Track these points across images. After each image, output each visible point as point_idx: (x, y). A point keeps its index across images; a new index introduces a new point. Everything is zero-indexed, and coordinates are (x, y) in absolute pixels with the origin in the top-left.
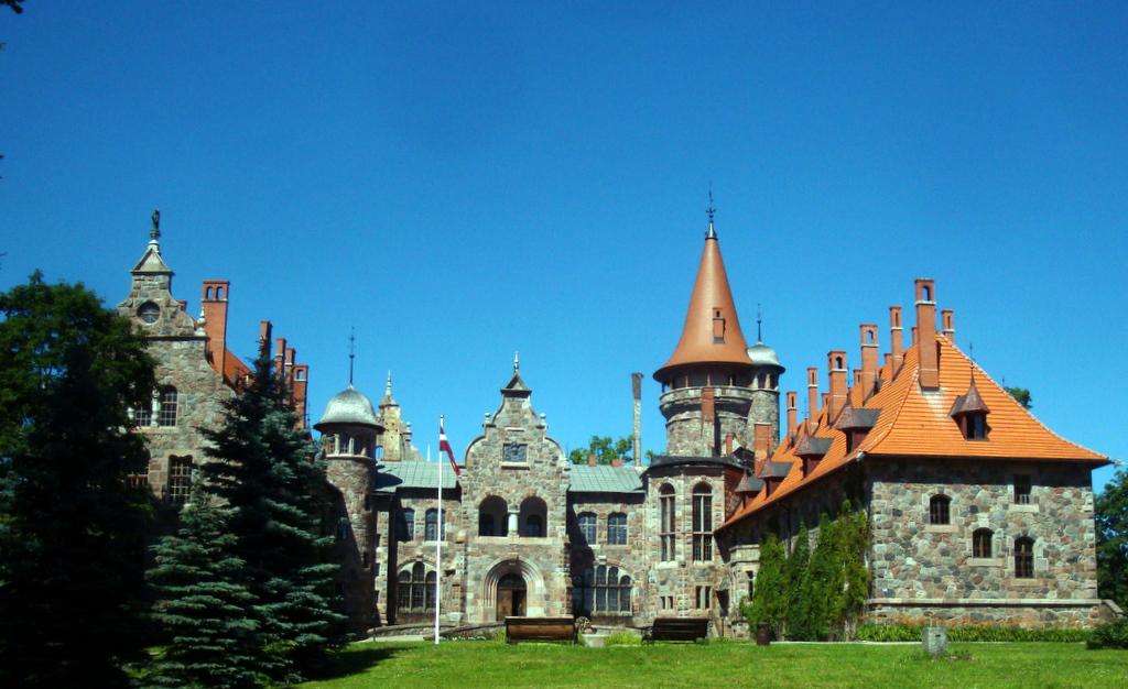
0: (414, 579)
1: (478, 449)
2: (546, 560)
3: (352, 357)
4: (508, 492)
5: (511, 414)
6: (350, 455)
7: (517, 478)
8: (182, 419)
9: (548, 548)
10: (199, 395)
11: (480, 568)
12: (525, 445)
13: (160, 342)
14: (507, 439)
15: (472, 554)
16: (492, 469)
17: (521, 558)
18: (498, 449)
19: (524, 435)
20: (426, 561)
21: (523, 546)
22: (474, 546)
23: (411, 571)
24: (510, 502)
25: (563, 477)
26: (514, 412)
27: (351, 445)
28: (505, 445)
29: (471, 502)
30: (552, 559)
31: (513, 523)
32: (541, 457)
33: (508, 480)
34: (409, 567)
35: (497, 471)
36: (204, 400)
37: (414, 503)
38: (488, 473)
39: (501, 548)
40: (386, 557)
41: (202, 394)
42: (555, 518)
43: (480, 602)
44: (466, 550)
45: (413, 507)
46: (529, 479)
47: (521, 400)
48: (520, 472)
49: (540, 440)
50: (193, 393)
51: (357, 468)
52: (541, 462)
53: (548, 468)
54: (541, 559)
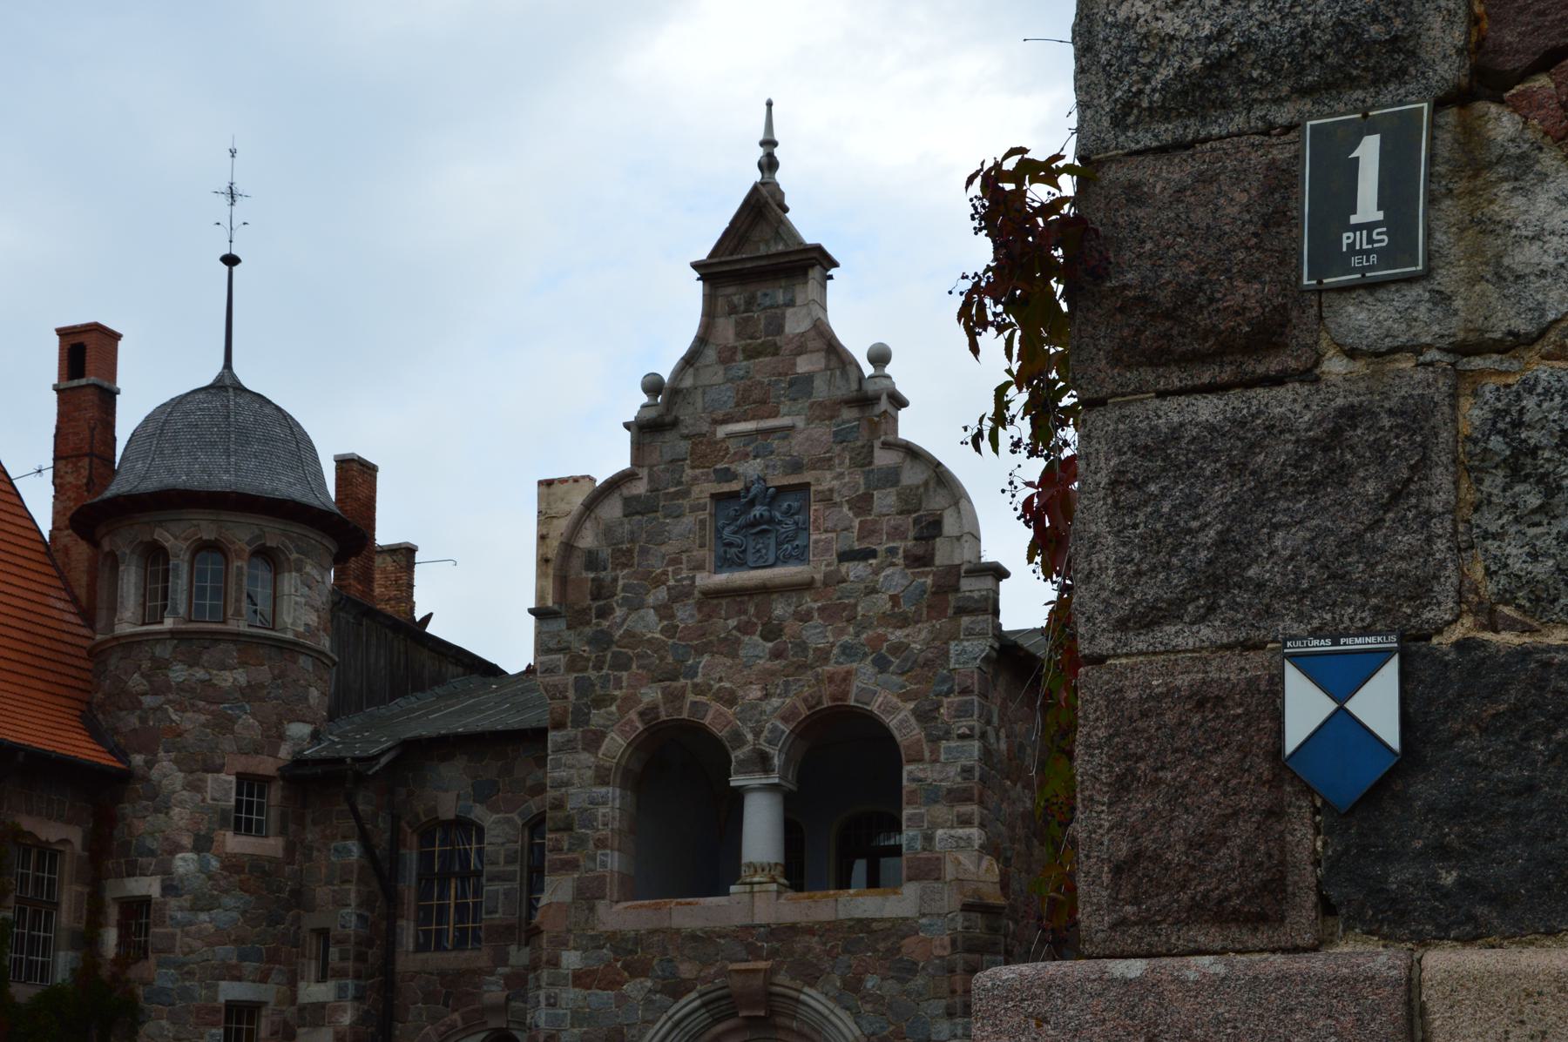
1: (608, 532)
2: (891, 987)
4: (730, 699)
5: (741, 365)
6: (169, 623)
7: (765, 638)
9: (899, 929)
12: (805, 487)
14: (727, 475)
15: (581, 979)
16: (664, 611)
19: (797, 446)
21: (793, 929)
22: (596, 942)
24: (738, 739)
25: (961, 611)
26: (751, 354)
27: (180, 584)
28: (716, 497)
29: (586, 758)
30: (919, 981)
32: (867, 532)
33: (730, 646)
35: (685, 615)
38: (649, 624)
39: (701, 941)
42: (932, 795)
44: (555, 963)
47: (780, 297)
48: (780, 609)
49: (864, 459)
51: (200, 674)
52: (873, 554)
53: (895, 578)
54: (871, 982)
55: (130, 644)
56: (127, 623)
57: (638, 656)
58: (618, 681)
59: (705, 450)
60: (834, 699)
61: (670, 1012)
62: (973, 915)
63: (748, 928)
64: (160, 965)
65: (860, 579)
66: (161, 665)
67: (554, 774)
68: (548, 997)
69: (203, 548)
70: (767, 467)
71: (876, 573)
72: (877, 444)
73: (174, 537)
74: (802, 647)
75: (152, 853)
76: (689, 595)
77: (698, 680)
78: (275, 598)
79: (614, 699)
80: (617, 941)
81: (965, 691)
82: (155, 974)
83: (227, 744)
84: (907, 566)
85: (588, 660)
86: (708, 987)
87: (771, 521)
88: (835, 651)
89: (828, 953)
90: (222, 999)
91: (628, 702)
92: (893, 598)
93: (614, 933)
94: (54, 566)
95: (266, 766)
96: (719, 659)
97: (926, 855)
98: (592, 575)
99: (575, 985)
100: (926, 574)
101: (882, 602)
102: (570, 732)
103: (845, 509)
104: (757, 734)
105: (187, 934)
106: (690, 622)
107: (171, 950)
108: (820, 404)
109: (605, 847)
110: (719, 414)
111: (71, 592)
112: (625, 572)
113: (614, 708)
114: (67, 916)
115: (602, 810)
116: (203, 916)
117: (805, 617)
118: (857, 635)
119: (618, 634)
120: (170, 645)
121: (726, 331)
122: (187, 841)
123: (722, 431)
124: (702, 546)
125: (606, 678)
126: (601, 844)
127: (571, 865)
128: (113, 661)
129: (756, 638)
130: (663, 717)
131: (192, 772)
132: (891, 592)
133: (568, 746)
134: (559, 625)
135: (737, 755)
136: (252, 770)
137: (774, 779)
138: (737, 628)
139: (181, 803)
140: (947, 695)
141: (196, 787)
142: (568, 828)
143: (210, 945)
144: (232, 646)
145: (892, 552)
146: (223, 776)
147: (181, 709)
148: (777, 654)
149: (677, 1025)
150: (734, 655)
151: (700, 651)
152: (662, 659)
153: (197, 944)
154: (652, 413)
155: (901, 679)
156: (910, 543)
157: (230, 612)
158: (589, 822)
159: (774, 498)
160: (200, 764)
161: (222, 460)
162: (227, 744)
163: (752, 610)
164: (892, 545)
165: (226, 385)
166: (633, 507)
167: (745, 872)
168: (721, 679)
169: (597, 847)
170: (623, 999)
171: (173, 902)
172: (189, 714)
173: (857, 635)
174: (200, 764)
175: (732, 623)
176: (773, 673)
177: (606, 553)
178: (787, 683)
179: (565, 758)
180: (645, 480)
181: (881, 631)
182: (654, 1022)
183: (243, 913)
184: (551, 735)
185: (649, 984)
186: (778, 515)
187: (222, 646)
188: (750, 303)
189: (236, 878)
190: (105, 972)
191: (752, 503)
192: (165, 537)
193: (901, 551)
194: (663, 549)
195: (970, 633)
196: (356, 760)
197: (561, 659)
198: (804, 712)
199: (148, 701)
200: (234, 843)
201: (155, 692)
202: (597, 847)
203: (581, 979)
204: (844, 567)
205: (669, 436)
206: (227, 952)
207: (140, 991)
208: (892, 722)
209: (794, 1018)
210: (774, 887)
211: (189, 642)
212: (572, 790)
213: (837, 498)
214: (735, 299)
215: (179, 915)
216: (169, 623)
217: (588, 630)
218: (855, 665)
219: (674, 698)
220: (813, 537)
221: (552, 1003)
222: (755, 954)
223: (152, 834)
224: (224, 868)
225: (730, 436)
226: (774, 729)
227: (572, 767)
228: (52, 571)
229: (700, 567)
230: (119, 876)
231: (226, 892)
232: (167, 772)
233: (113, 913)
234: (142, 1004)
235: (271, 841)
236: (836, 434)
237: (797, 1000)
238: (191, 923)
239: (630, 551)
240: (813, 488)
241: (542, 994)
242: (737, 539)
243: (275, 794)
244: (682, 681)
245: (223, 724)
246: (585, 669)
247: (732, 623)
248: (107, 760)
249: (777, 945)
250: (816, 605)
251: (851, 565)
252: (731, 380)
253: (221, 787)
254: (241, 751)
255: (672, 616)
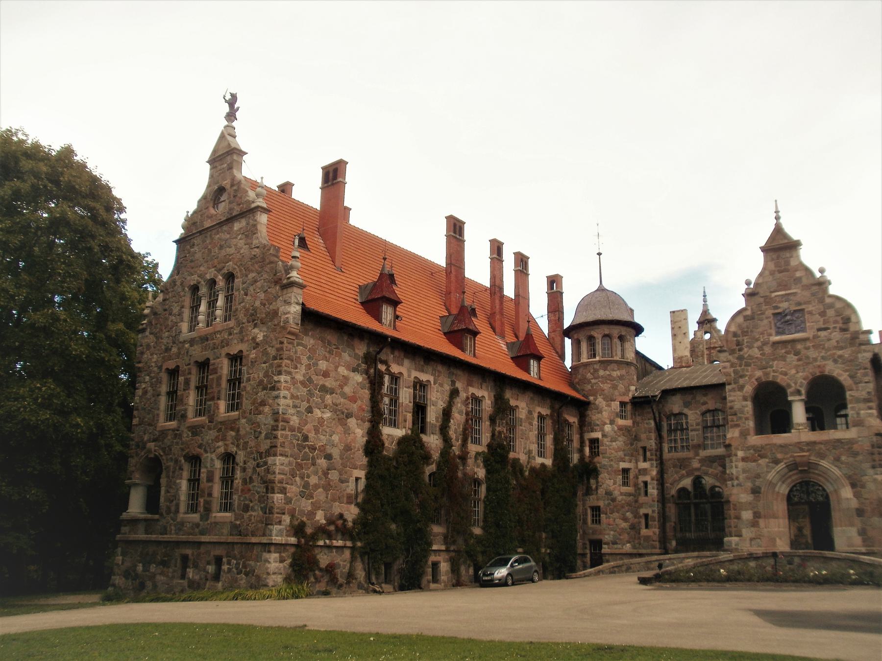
0: (696, 498)
1: (740, 326)
3: (599, 254)
4: (785, 374)
5: (778, 275)
6: (597, 359)
7: (795, 355)
8: (237, 310)
10: (251, 275)
11: (758, 476)
12: (803, 310)
13: (225, 228)
14: (776, 308)
15: (744, 459)
16: (760, 348)
17: (813, 459)
18: (766, 322)
19: (798, 298)
20: (706, 474)
21: (814, 443)
22: (749, 448)
23: (690, 488)
24: (789, 386)
26: (780, 272)
27: (599, 348)
28: (775, 315)
29: (739, 393)
31: (799, 414)
32: (825, 322)
33: (783, 358)
34: (687, 483)
35: (768, 349)
36: (256, 281)
37: (687, 405)
38: (756, 352)
39: (783, 447)
40: (654, 473)
41: (254, 275)
43: (762, 522)
44: (736, 455)
45: (686, 411)
46: (812, 353)
47: (788, 255)
48: (799, 346)
49: (821, 301)
50: (247, 276)
51: (608, 373)
53: (836, 336)
55: (586, 365)
56: (584, 359)
57: (753, 362)
58: (747, 371)
59: (768, 300)
60: (820, 372)
61: (776, 469)
62: (878, 437)
63: (799, 443)
64: (603, 457)
65: (826, 336)
66: (596, 371)
67: (729, 398)
68: (736, 465)
69: (605, 336)
70: (790, 304)
71: (830, 334)
72: (826, 296)
73: (597, 333)
74: (808, 357)
75: (598, 425)
76: (768, 343)
77: (774, 368)
78: (623, 351)
79: (747, 375)
80: (756, 449)
81: (865, 368)
82: (601, 461)
83: (616, 393)
84: (840, 332)
85: (736, 364)
86: (785, 461)
87: (792, 320)
88: (819, 358)
89: (828, 450)
90: (621, 468)
91: (751, 377)
92: (837, 342)
93: (754, 446)
94: (550, 343)
95: (627, 399)
96: (780, 362)
97: (857, 419)
98: (735, 339)
99: (742, 461)
100: (847, 334)
101: (833, 343)
102: (733, 386)
103: (817, 315)
104: (796, 384)
105: (610, 449)
106: (770, 351)
107: (605, 453)
108: (805, 285)
109: (748, 420)
110: (772, 290)
111: (556, 351)
112: (747, 337)
113: (747, 378)
114: (576, 444)
115: (746, 409)
116: (614, 443)
117: (807, 348)
118: (826, 353)
119: (746, 356)
120: (599, 364)
121: (772, 266)
122: (608, 422)
123: (774, 295)
124: (771, 328)
125: (744, 369)
126: (747, 419)
127: (737, 426)
128: (581, 370)
129: (792, 355)
130: (764, 380)
131: (608, 401)
132: (837, 340)
133: (733, 390)
134: (726, 354)
135: (789, 391)
136: (623, 400)
137: (803, 397)
138: (785, 353)
139: (605, 411)
140: (859, 370)
141: (609, 406)
142: (735, 414)
143: (616, 452)
144: (615, 364)
145: (835, 328)
146: (616, 402)
147: (603, 383)
148: (799, 360)
149: (778, 472)
150: (785, 361)
151: (773, 360)
152: (761, 363)
153: (613, 451)
154: (749, 291)
155: (843, 366)
156: (841, 325)
157: (614, 354)
158: (742, 412)
159: (793, 313)
160: (610, 399)
161: (609, 311)
162: (616, 393)
163: (790, 347)
164: (834, 325)
165: (601, 289)
166: (746, 318)
167: (795, 426)
168: (781, 368)
169: (746, 420)
170: (759, 465)
171: (605, 440)
172: (605, 385)
173: (826, 353)
174: (610, 399)
175: (783, 351)
176: (799, 366)
177: (739, 332)
178: (804, 368)
179: (732, 393)
180: (750, 310)
181: (834, 351)
182: (770, 472)
183: (624, 442)
184: (728, 387)
185: (767, 460)
186: (795, 319)
187: (613, 364)
188: (778, 258)
189: (621, 432)
190: (587, 460)
191: (786, 315)
192: (593, 333)
193: (838, 328)
194: (758, 330)
195: (865, 351)
196: (652, 396)
197: (728, 364)
198: (811, 377)
199: (593, 381)
200: (621, 422)
201: (595, 378)
202: (746, 420)
203: (744, 459)
204: (820, 333)
205: (756, 297)
206: (621, 454)
207: (598, 465)
208: (841, 379)
209: (817, 469)
210: (807, 430)
211: (604, 364)
212: (736, 403)
213: (814, 312)
214: (774, 256)
215: (607, 443)
216: (597, 359)
217: (736, 355)
218: (826, 362)
219: (766, 374)
220: (808, 324)
221: (736, 467)
222: (802, 450)
223: (598, 420)
224: (618, 429)
225: (776, 296)
226: (801, 383)
227: (735, 396)
228: (549, 344)
229: (770, 335)
230: (588, 432)
231: (619, 436)
232: (600, 401)
233: (587, 443)
234: (599, 469)
235: (629, 421)
236: (812, 294)
237: (819, 464)
238: (611, 446)
239: (747, 332)
240: (806, 310)
241: (733, 465)
242: (781, 326)
243: (629, 407)
244: (769, 369)
245: (615, 387)
246: (736, 367)
247: (783, 351)
248: (582, 398)
249: (810, 447)
250: (811, 345)
251: (821, 332)
252: (775, 280)
253: (616, 405)
254: (620, 395)
255: (763, 350)
